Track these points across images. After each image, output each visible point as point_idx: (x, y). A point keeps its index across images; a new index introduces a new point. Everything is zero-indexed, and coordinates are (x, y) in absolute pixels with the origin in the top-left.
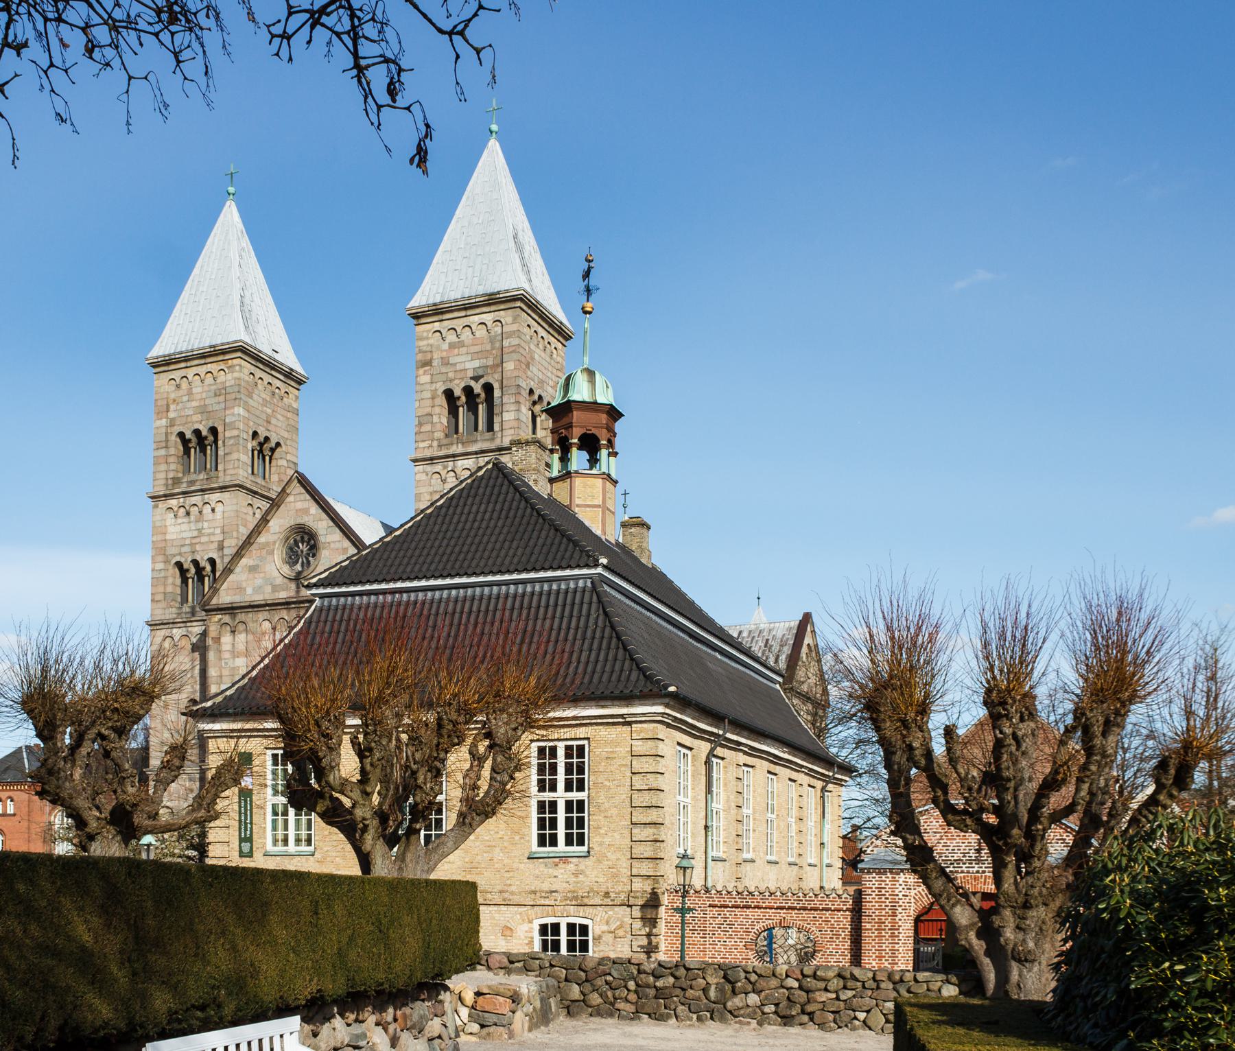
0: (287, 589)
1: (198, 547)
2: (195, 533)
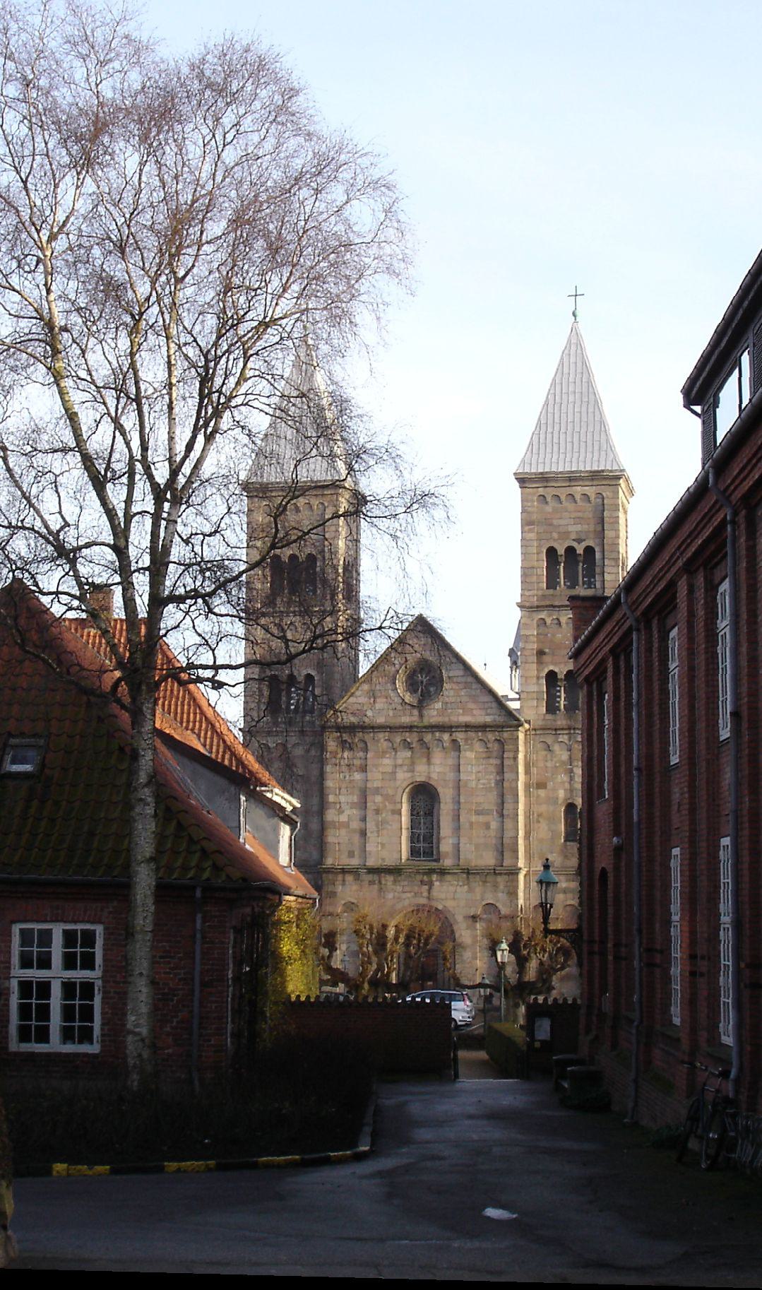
0: (411, 715)
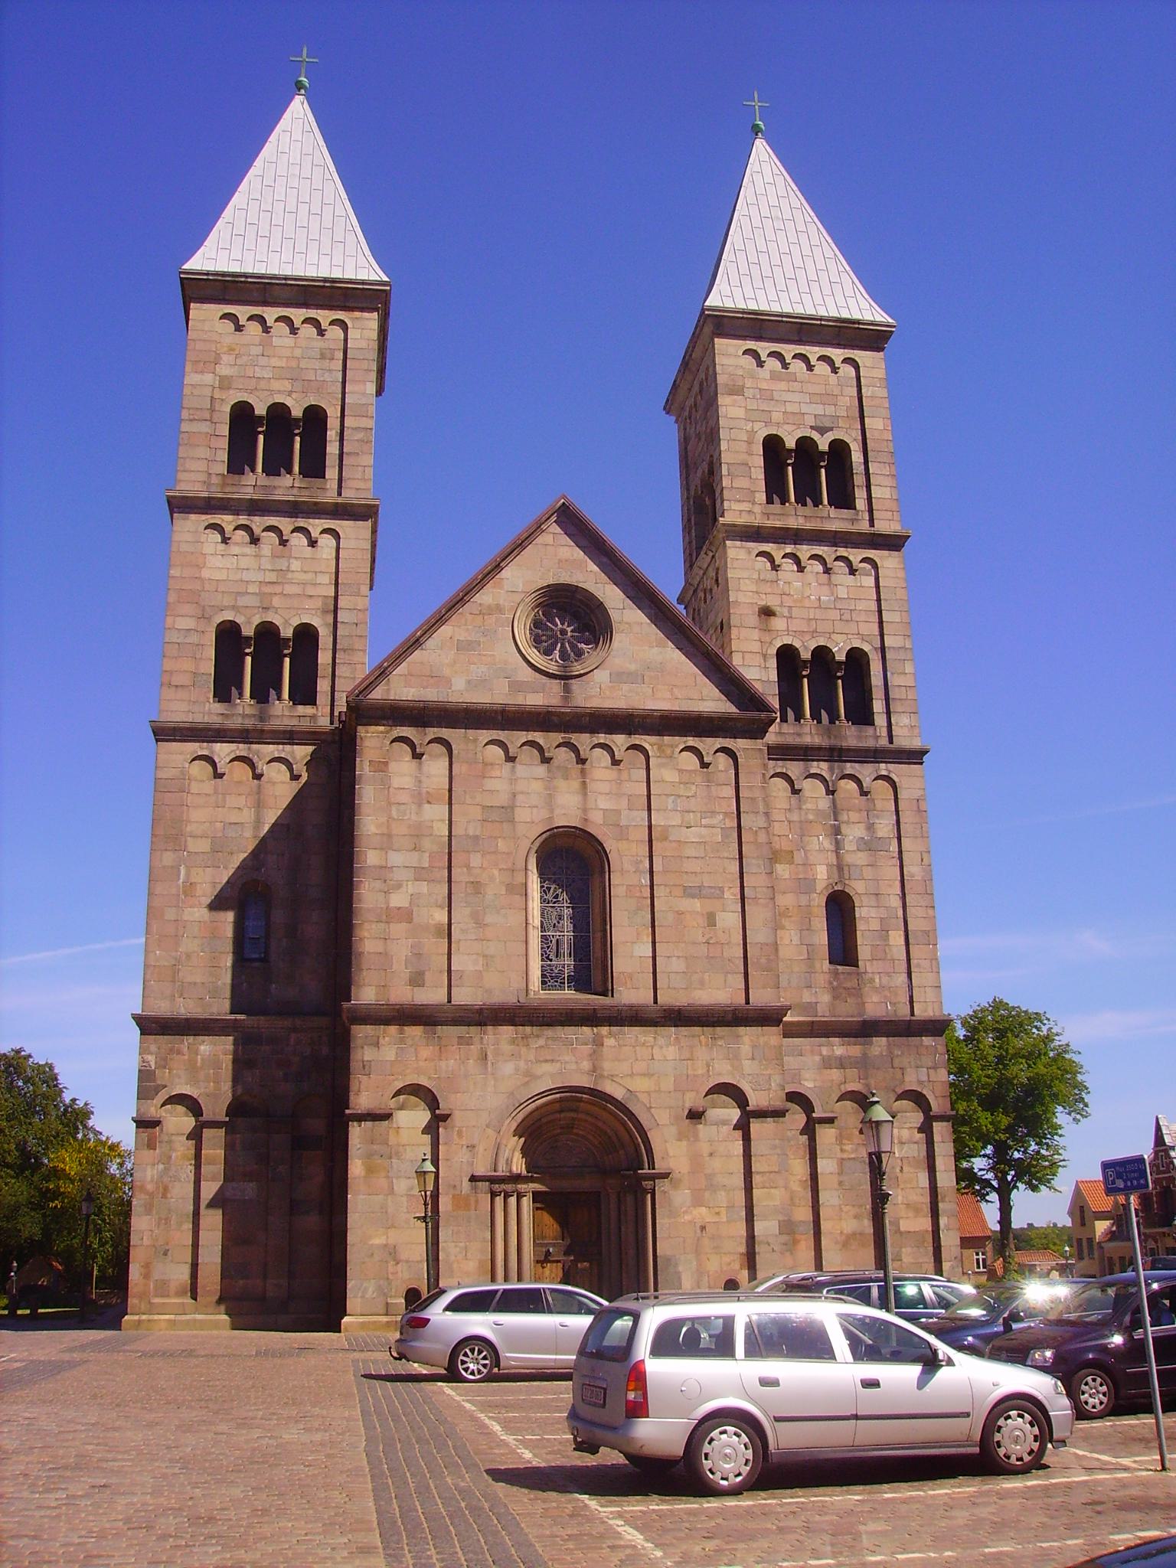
1: (276, 602)
2: (272, 577)
